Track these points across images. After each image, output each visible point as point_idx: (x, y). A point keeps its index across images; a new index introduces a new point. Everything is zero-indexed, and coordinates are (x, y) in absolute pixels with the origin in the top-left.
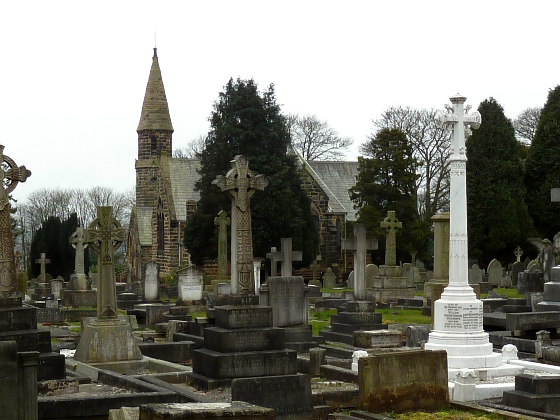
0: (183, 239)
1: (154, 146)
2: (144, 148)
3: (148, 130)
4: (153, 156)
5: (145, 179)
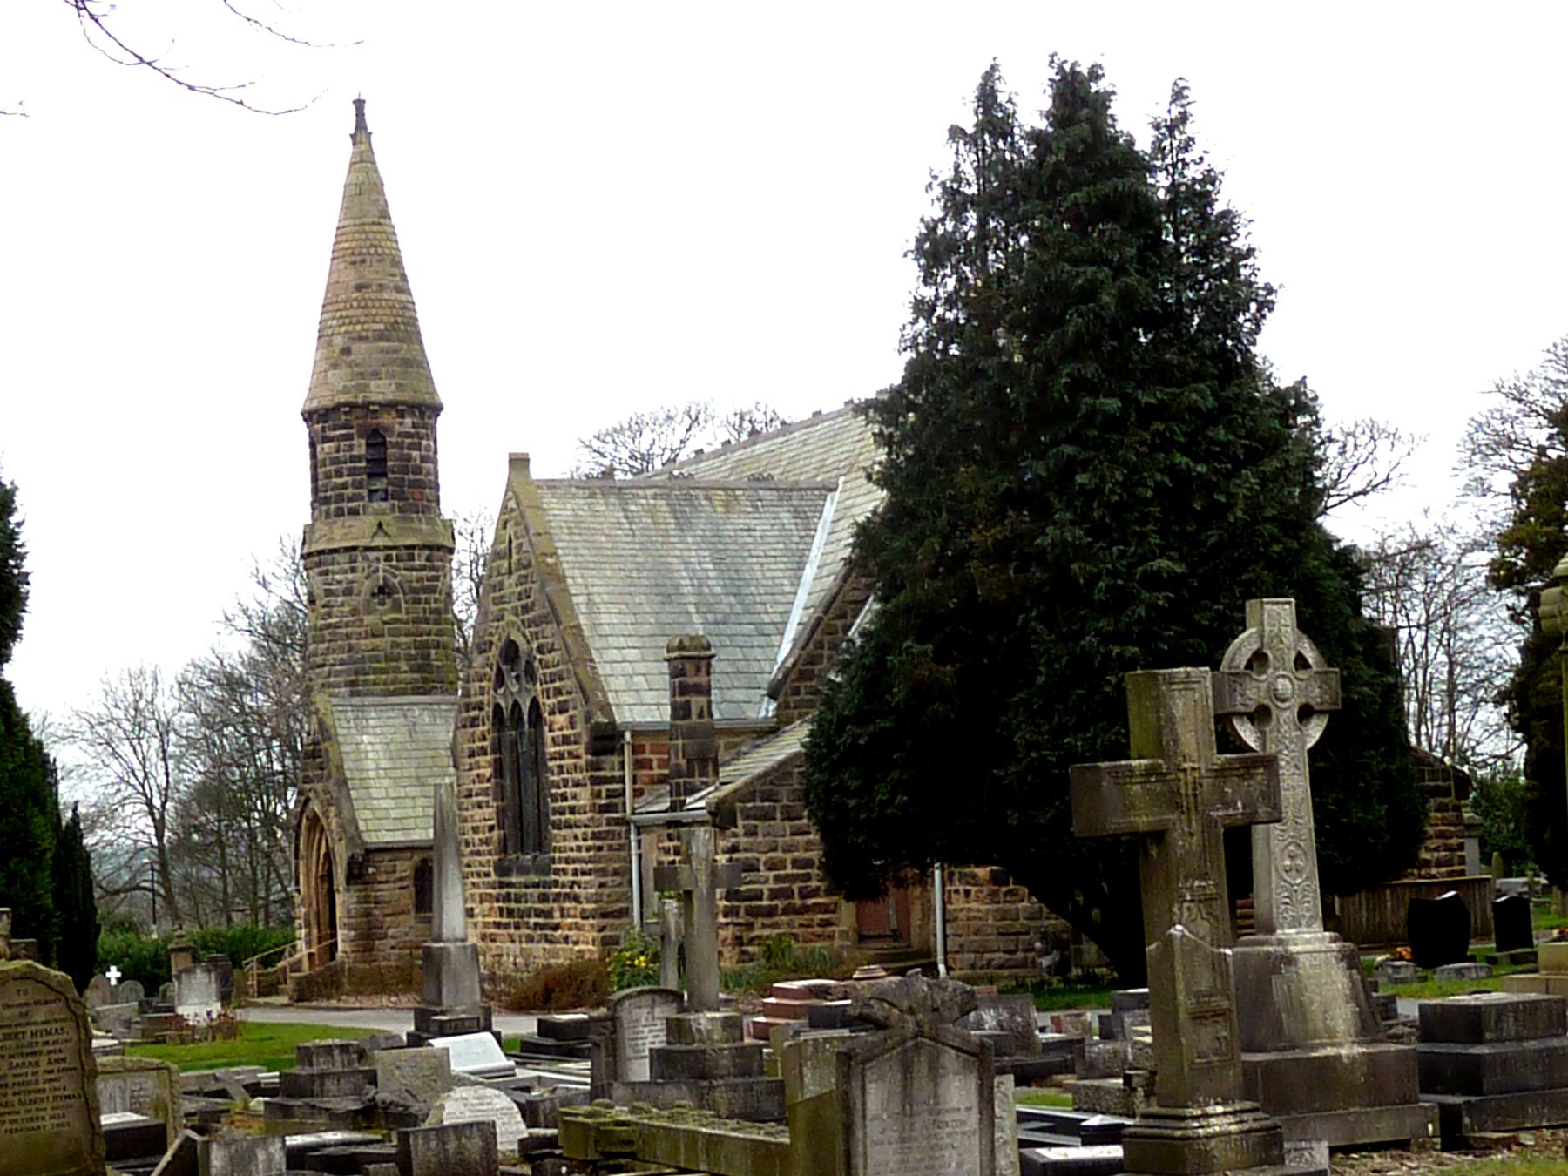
0: (1315, 731)
1: (377, 468)
2: (339, 474)
3: (353, 406)
4: (375, 505)
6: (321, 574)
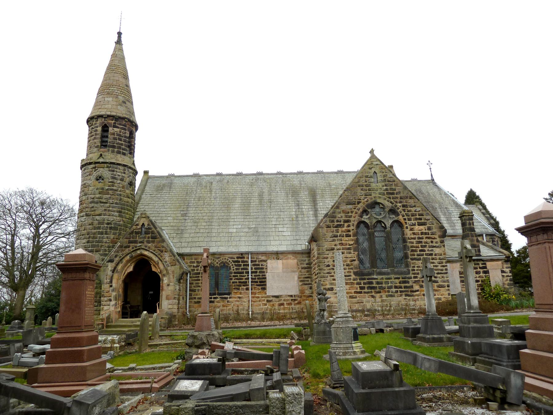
2: (120, 140)
5: (122, 180)
6: (109, 171)
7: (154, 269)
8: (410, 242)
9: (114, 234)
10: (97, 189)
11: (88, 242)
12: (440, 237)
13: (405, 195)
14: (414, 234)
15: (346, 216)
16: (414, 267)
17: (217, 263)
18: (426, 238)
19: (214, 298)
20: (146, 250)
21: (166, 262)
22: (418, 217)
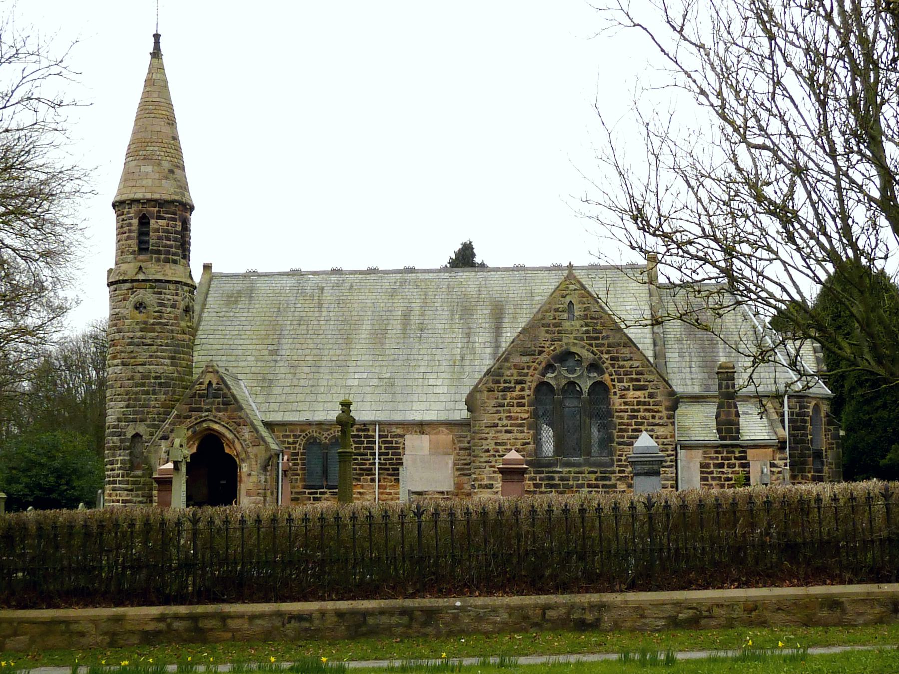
2: (168, 239)
5: (174, 306)
6: (155, 293)
7: (227, 450)
8: (618, 417)
9: (165, 394)
10: (137, 323)
11: (127, 407)
12: (667, 409)
13: (616, 340)
14: (626, 404)
15: (520, 375)
16: (621, 455)
17: (326, 438)
18: (646, 410)
19: (321, 493)
20: (216, 423)
21: (245, 441)
22: (634, 376)
